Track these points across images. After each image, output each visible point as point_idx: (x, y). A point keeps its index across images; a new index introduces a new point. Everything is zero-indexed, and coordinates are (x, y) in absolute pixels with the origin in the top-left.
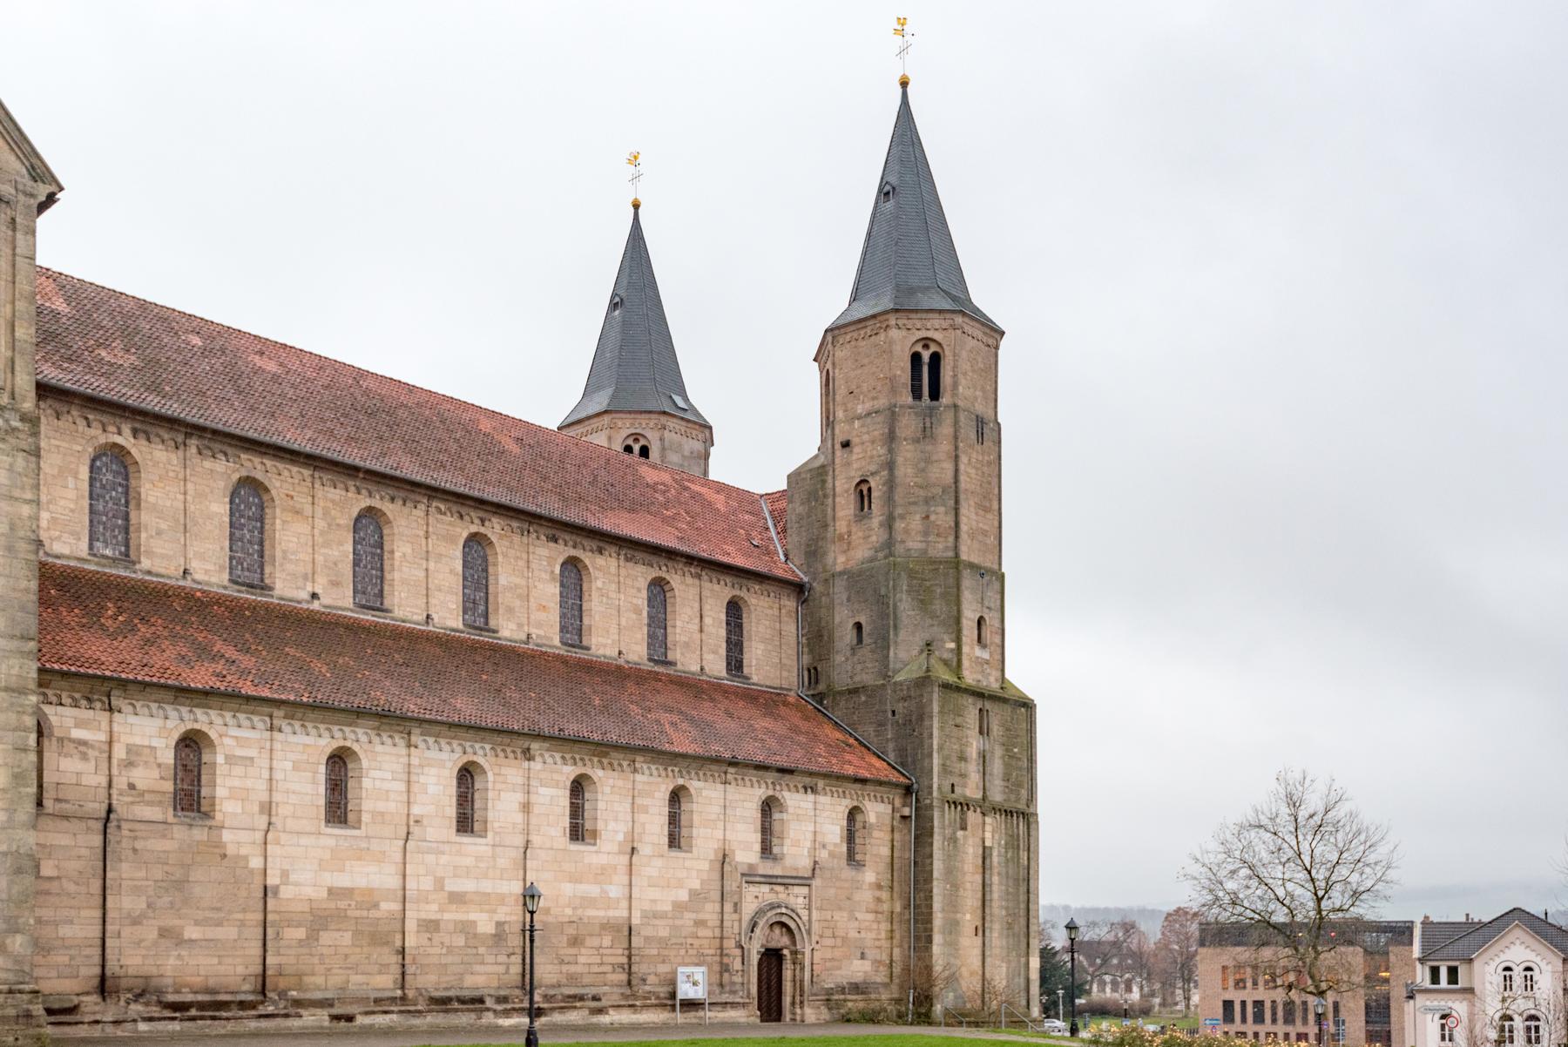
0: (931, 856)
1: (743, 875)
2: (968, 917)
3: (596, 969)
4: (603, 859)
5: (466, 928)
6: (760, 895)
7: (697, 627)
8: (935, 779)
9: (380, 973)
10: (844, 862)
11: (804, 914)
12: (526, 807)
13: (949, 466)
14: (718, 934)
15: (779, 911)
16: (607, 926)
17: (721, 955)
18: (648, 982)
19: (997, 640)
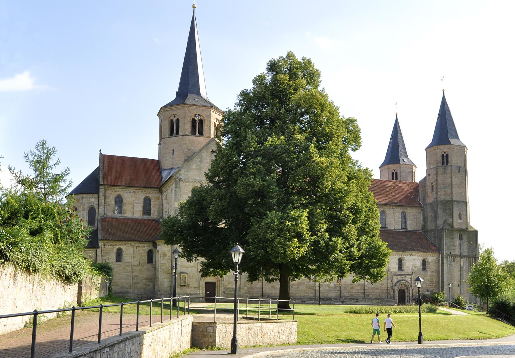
0: (444, 268)
1: (393, 274)
2: (456, 282)
7: (393, 219)
8: (445, 251)
9: (311, 294)
10: (421, 271)
11: (410, 282)
13: (450, 179)
14: (387, 286)
17: (388, 291)
19: (465, 217)
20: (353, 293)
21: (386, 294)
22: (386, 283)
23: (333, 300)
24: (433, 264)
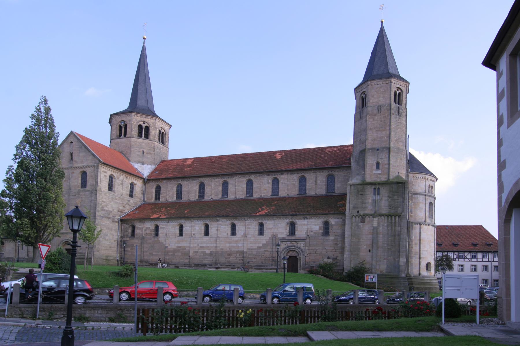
1: (280, 240)
3: (235, 260)
4: (237, 239)
5: (204, 253)
6: (287, 244)
12: (217, 230)
15: (291, 247)
16: (238, 252)
20: (230, 260)
21: (271, 261)
22: (271, 249)
23: (207, 266)
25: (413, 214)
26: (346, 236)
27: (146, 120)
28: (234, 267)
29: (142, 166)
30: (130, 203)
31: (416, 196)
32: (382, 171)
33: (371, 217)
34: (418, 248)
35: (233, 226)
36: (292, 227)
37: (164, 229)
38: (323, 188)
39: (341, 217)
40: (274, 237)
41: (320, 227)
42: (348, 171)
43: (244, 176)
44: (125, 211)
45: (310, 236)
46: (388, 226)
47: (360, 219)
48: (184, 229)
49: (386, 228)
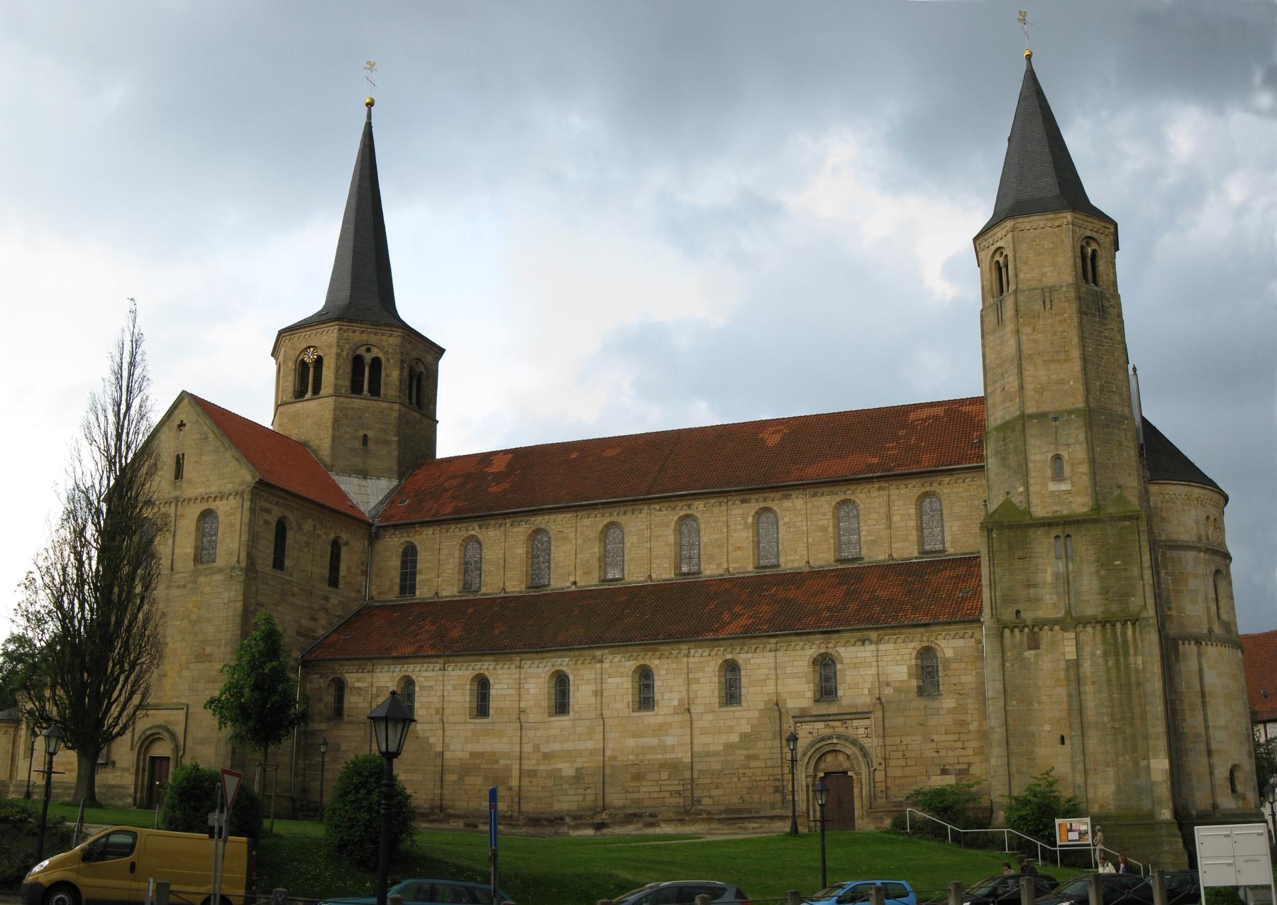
1: (793, 717)
3: (656, 795)
4: (660, 719)
5: (555, 775)
6: (815, 732)
10: (913, 695)
12: (599, 693)
16: (663, 765)
18: (703, 802)
20: (641, 796)
23: (567, 820)
24: (963, 665)
25: (1173, 613)
26: (990, 694)
27: (373, 339)
28: (652, 820)
29: (364, 482)
30: (329, 606)
31: (1175, 553)
32: (1073, 484)
33: (1057, 628)
34: (1201, 719)
35: (645, 677)
36: (825, 667)
37: (432, 693)
38: (911, 538)
39: (970, 632)
40: (777, 706)
41: (909, 668)
42: (979, 483)
43: (673, 504)
44: (314, 631)
45: (883, 700)
46: (1105, 655)
47: (1026, 636)
48: (492, 692)
49: (1101, 660)
